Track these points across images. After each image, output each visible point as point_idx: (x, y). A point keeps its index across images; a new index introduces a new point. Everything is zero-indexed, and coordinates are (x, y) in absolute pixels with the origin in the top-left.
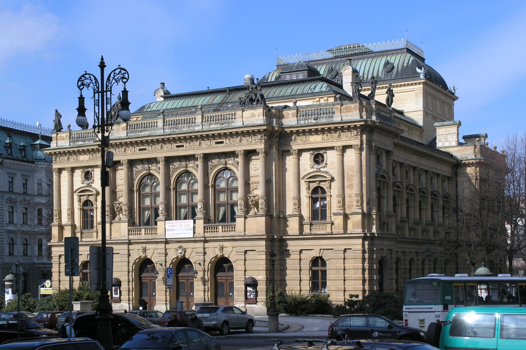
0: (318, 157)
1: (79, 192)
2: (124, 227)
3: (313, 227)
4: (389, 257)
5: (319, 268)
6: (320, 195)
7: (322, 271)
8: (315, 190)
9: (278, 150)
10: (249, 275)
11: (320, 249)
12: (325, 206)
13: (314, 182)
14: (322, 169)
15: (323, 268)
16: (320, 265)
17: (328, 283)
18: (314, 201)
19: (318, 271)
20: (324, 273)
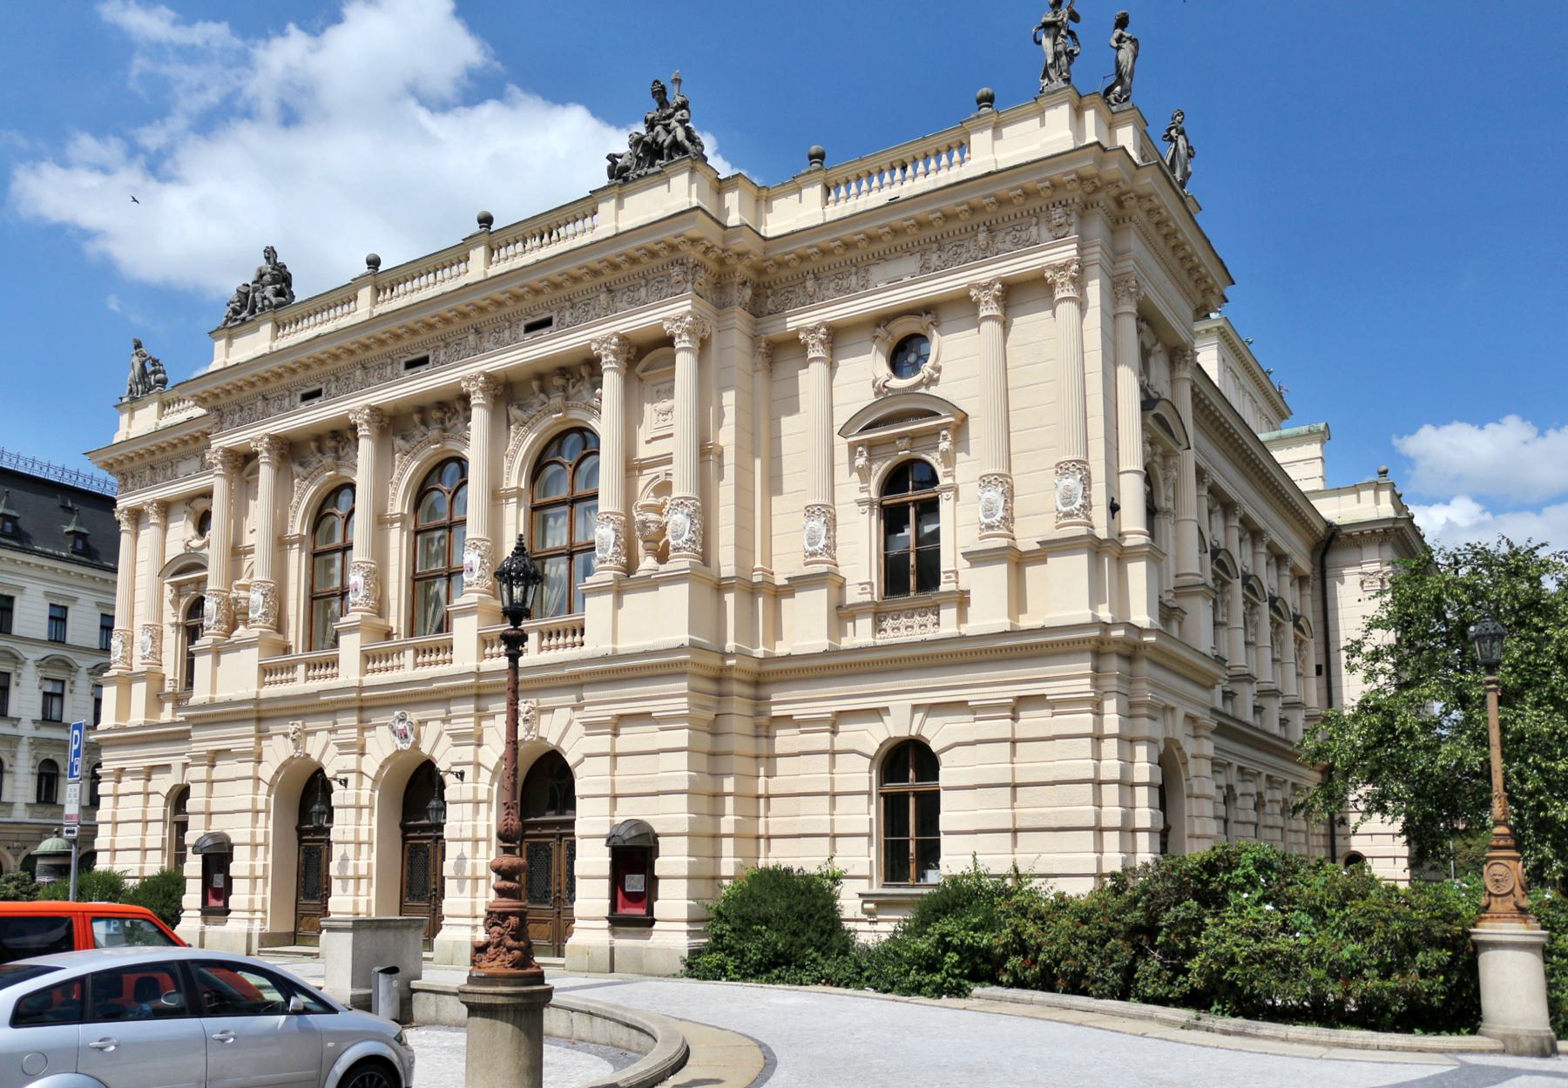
0: (905, 353)
1: (174, 575)
2: (250, 660)
3: (889, 623)
4: (1190, 747)
5: (912, 784)
6: (911, 495)
7: (916, 794)
8: (895, 480)
9: (754, 338)
10: (629, 810)
11: (916, 708)
12: (937, 531)
13: (890, 441)
14: (923, 390)
15: (926, 786)
16: (912, 774)
17: (945, 841)
18: (893, 519)
19: (905, 796)
20: (930, 805)
